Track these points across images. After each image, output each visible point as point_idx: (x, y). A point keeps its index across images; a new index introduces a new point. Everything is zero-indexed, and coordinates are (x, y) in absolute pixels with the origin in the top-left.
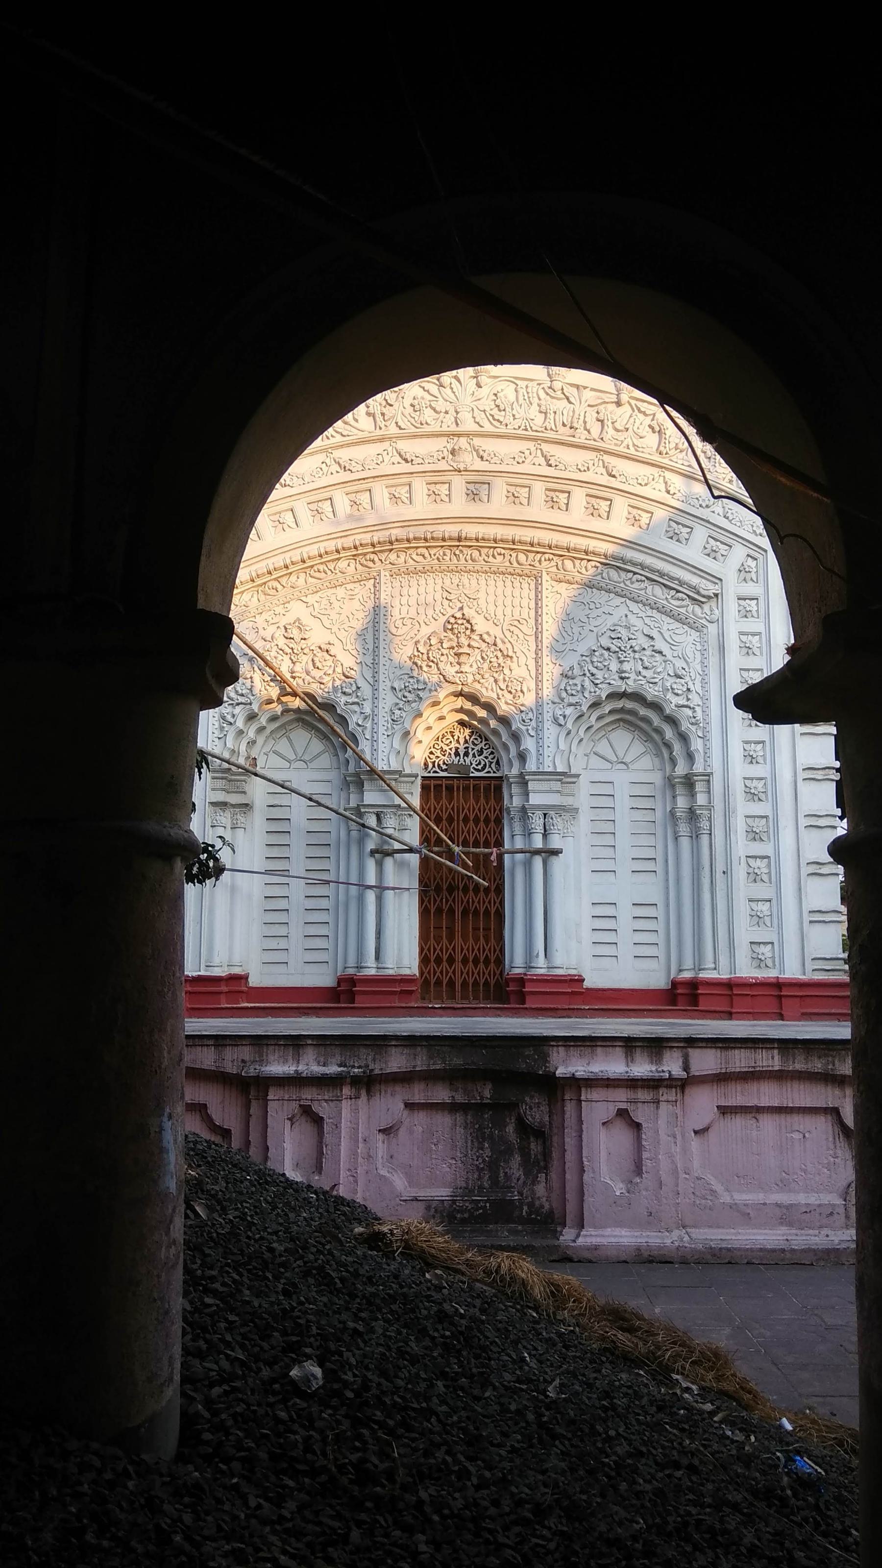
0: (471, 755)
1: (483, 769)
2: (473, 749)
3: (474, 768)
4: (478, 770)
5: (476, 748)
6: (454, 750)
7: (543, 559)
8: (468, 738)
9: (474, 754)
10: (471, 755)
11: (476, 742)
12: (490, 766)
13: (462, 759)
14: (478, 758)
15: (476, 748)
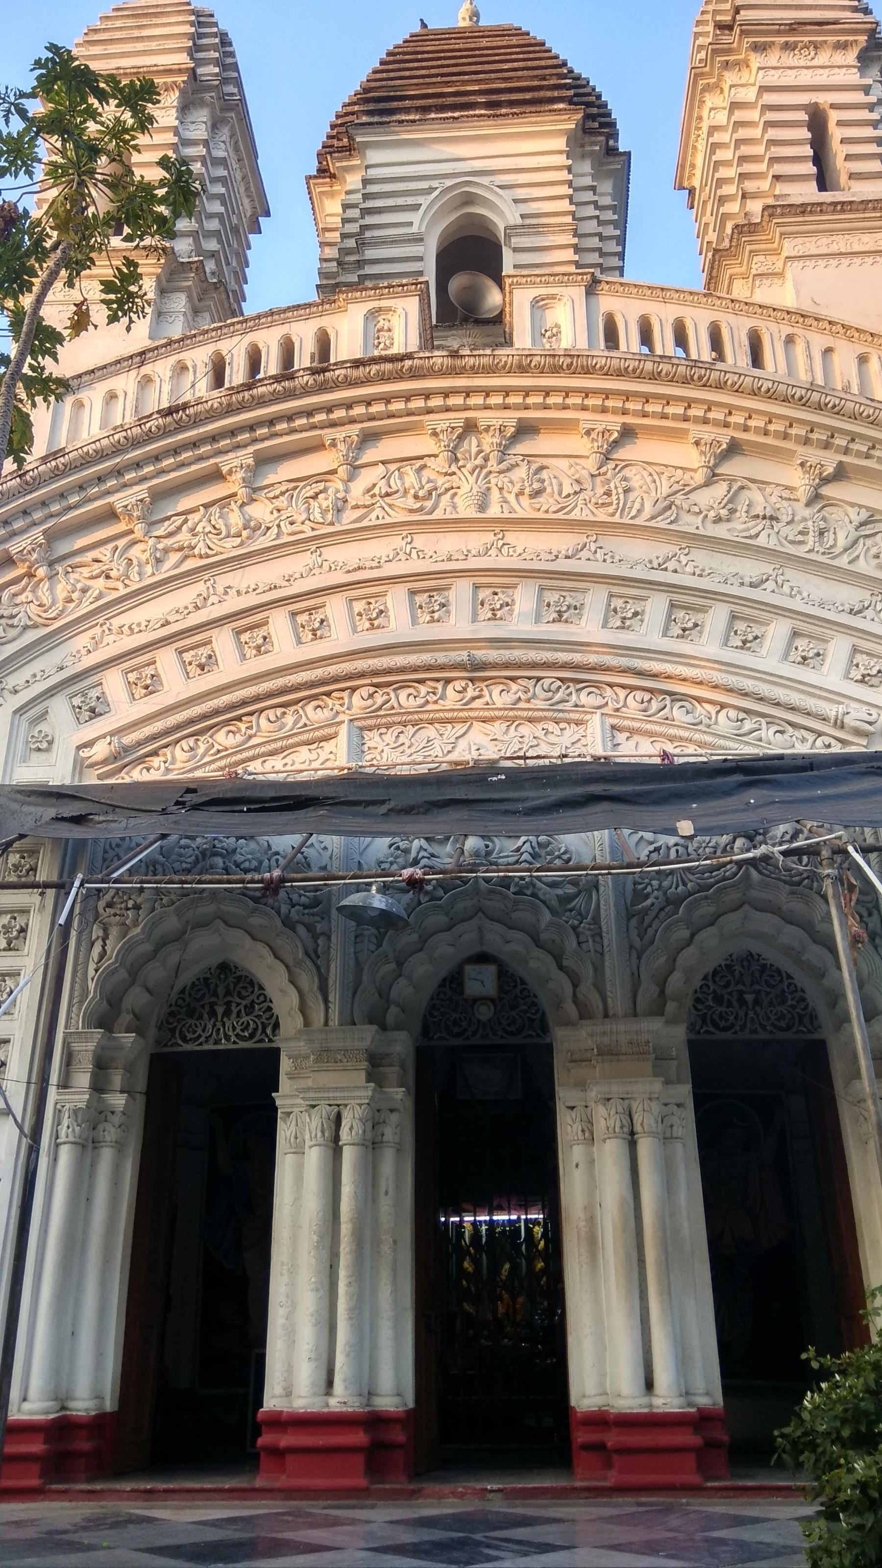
0: (234, 1015)
1: (252, 1036)
2: (238, 1004)
3: (237, 1035)
4: (244, 1039)
5: (244, 1003)
6: (207, 1008)
7: (150, 273)
8: (231, 986)
9: (239, 1012)
10: (234, 1015)
11: (244, 993)
12: (264, 1031)
13: (219, 1025)
14: (245, 1019)
15: (244, 1003)
